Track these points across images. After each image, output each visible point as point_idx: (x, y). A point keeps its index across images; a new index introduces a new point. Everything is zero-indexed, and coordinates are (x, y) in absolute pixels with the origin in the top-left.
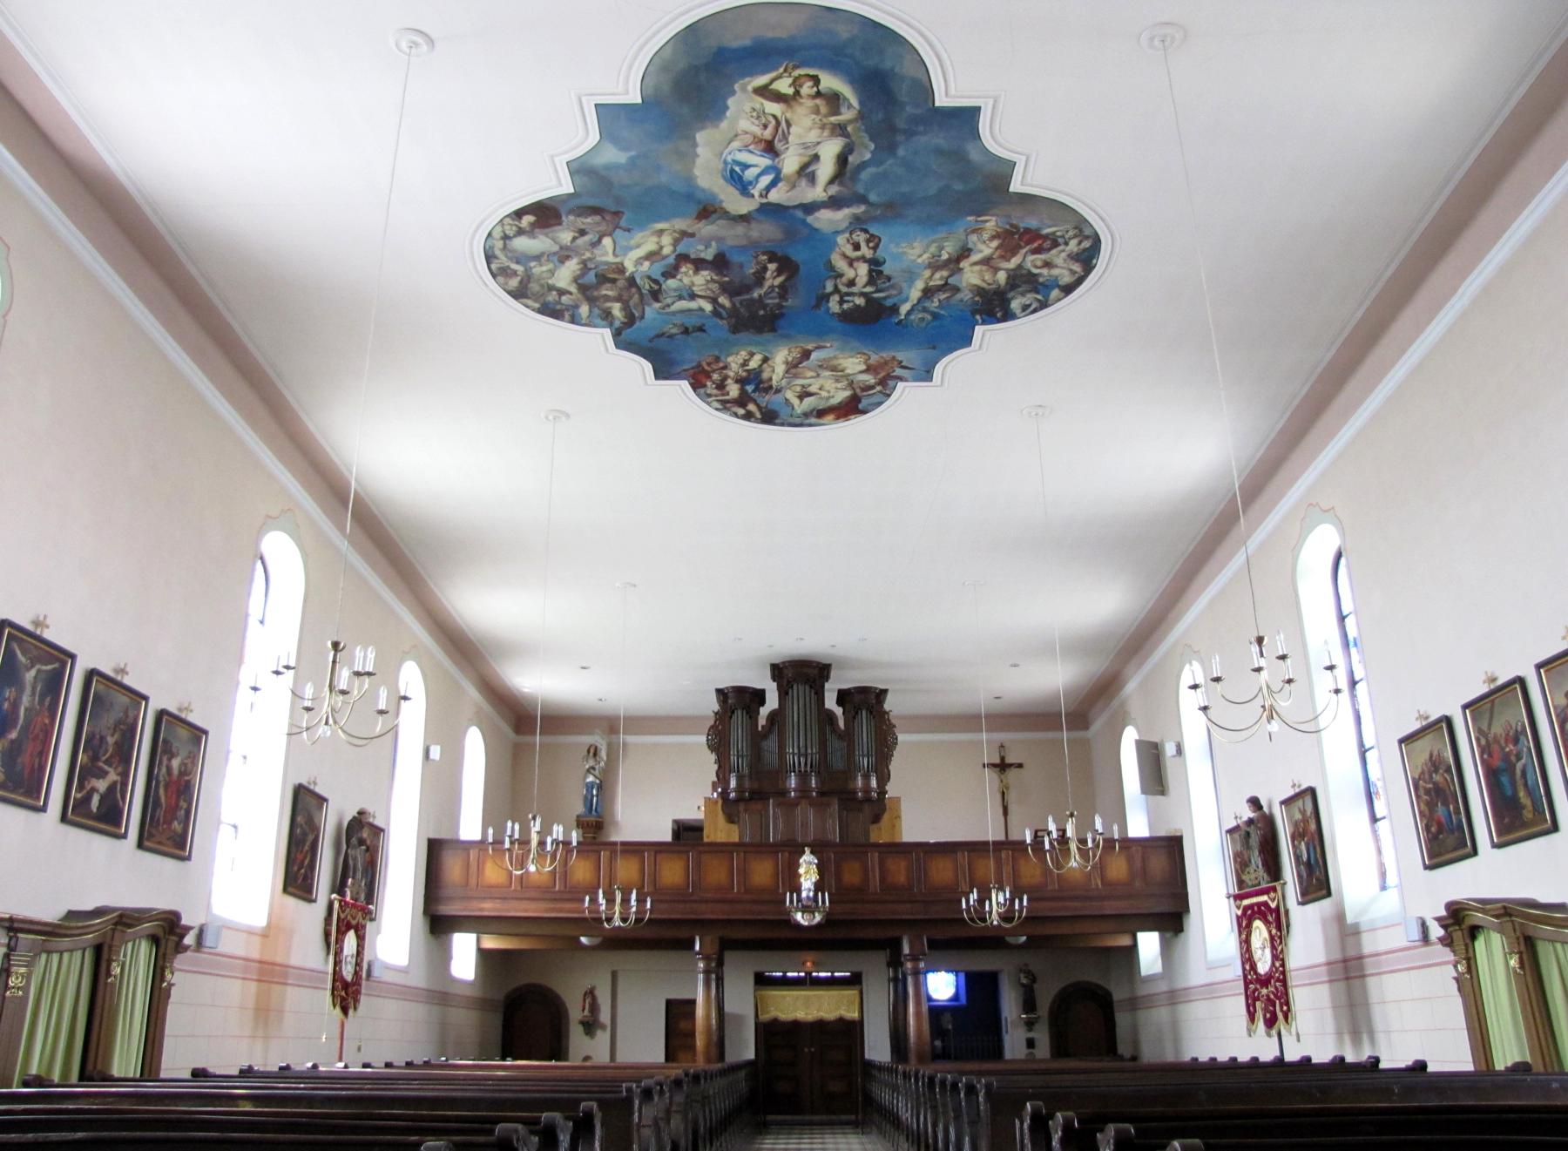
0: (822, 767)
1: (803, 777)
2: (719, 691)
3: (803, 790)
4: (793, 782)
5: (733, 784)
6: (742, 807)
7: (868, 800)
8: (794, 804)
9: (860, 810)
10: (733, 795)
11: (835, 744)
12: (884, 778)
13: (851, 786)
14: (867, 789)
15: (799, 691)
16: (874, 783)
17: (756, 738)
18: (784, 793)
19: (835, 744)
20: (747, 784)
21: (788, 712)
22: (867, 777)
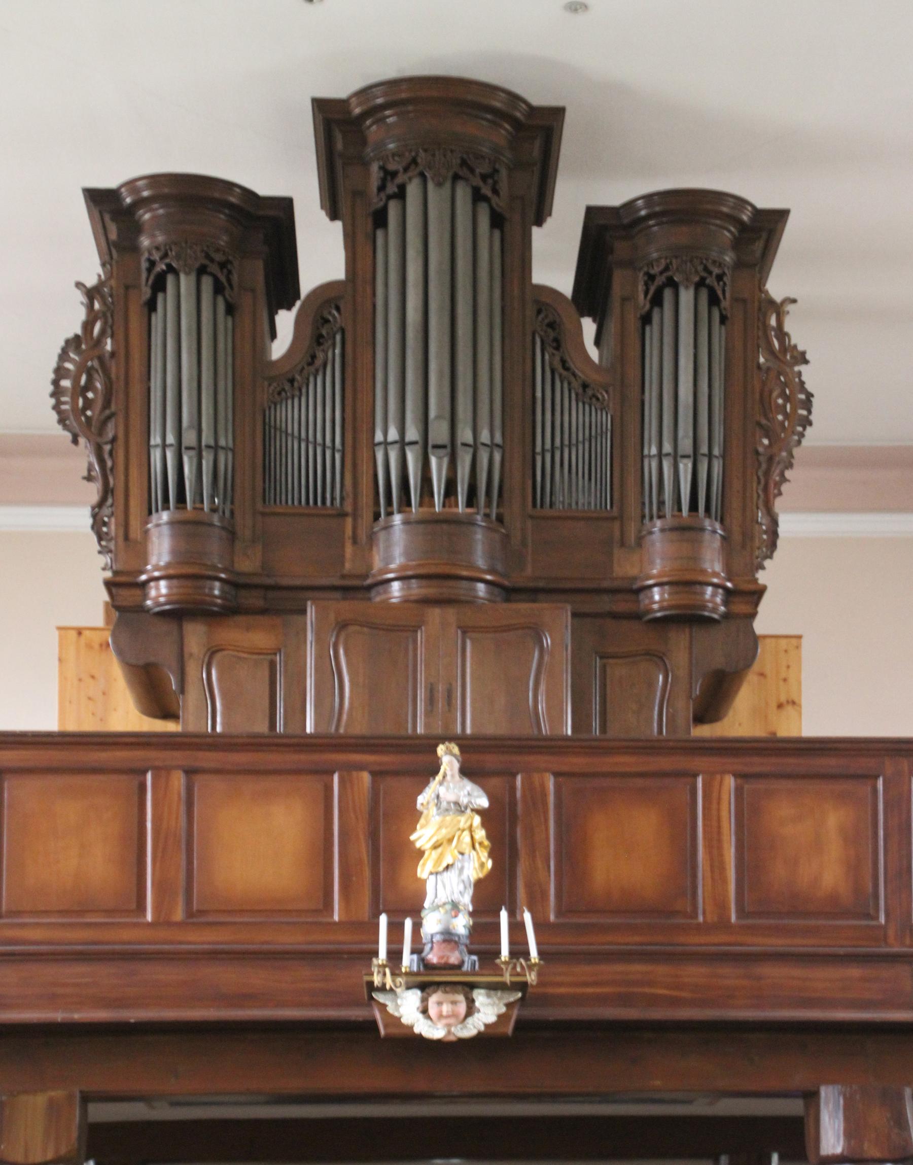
0: (514, 493)
1: (440, 530)
2: (100, 200)
3: (440, 584)
4: (395, 547)
5: (161, 549)
6: (195, 636)
7: (689, 618)
8: (399, 628)
9: (659, 658)
10: (160, 592)
11: (570, 422)
12: (753, 542)
13: (625, 567)
14: (686, 583)
15: (432, 212)
16: (713, 563)
17: (257, 392)
18: (361, 587)
19: (570, 422)
20: (214, 550)
21: (386, 292)
22: (687, 531)
